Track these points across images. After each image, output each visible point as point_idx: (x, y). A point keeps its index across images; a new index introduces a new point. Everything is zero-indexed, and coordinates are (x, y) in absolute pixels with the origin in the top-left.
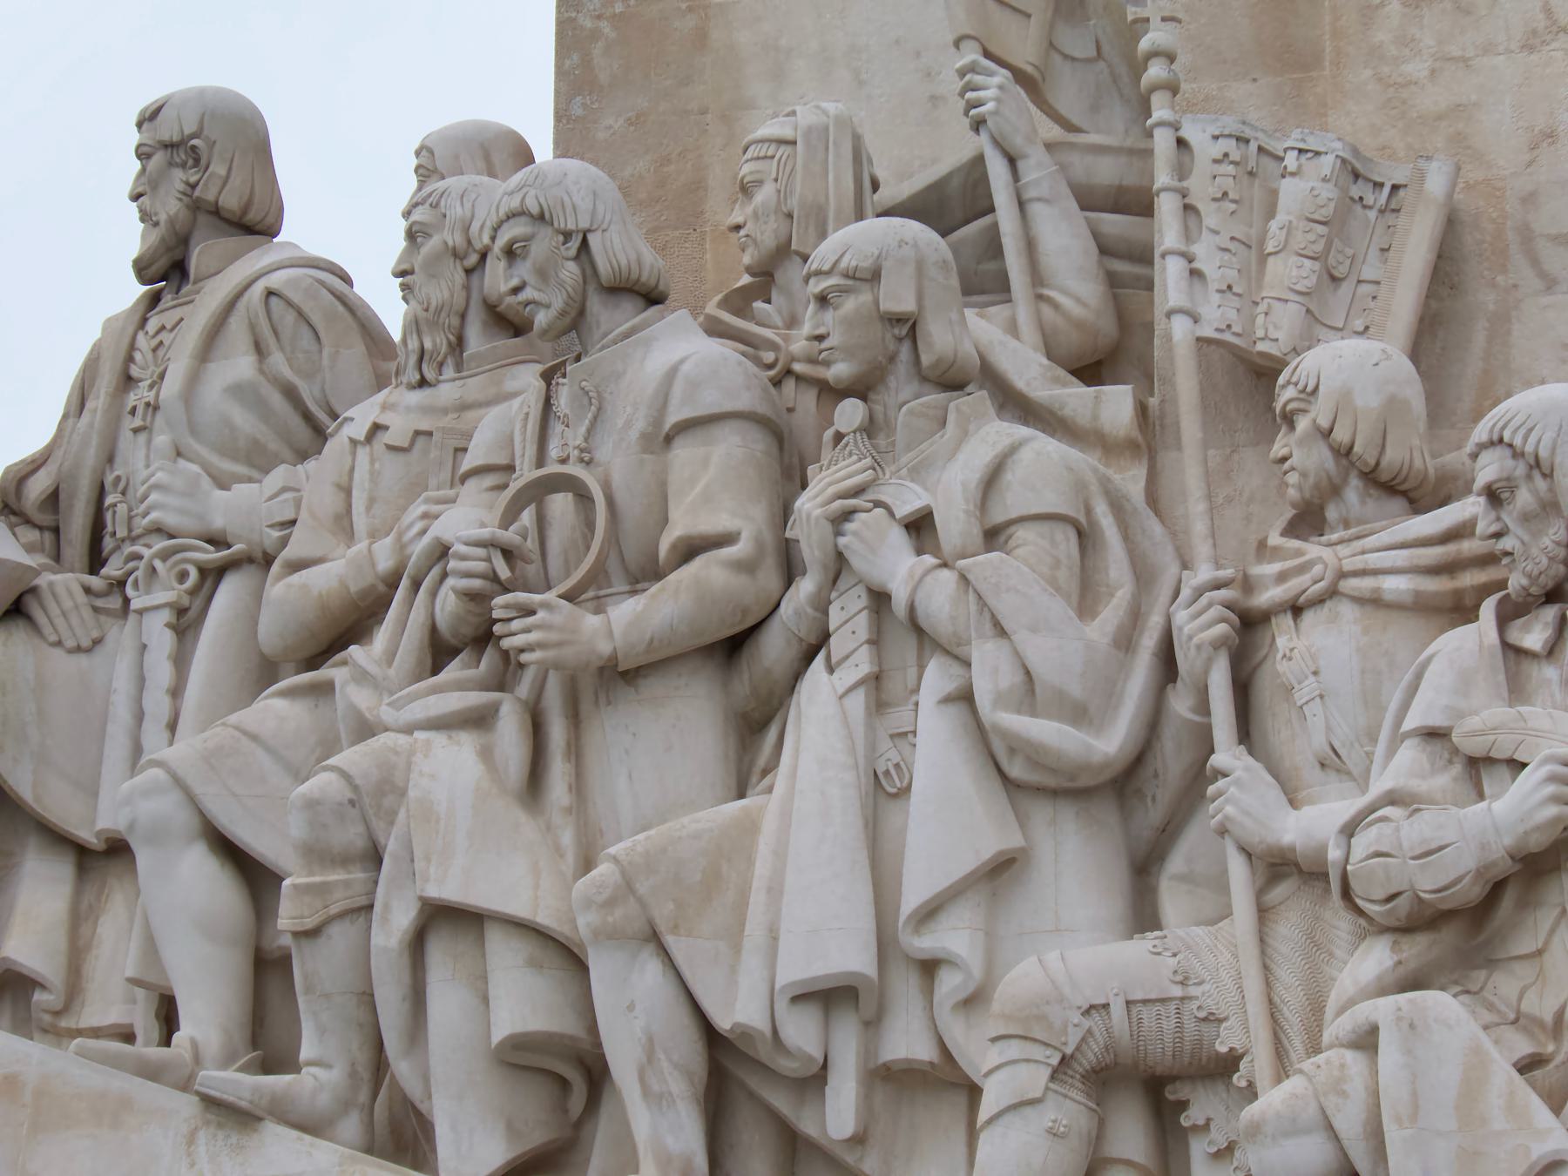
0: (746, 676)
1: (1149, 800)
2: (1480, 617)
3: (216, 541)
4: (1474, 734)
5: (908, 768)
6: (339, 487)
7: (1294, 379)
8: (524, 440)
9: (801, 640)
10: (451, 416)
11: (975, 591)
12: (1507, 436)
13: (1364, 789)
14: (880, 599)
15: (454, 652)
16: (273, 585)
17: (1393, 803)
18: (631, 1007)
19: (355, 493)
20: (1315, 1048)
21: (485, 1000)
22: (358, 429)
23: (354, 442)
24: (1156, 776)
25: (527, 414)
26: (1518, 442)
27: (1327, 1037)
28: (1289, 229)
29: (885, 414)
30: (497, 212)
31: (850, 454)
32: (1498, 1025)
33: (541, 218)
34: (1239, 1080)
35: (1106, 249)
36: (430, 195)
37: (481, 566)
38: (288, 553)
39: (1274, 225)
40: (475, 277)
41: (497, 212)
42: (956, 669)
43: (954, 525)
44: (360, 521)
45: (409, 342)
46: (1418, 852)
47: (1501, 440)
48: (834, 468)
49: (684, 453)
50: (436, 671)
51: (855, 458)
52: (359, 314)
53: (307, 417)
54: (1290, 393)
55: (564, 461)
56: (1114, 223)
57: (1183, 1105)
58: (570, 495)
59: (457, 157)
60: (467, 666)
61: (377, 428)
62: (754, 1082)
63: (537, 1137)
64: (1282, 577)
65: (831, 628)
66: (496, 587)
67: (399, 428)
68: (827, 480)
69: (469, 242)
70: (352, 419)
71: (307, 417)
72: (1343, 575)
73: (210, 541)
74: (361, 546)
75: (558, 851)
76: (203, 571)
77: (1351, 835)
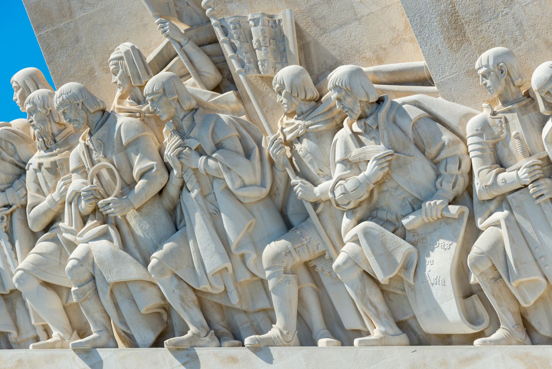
0: (167, 199)
1: (278, 195)
2: (344, 126)
3: (8, 206)
4: (354, 156)
5: (218, 209)
6: (34, 182)
7: (277, 82)
8: (85, 158)
9: (178, 186)
10: (59, 155)
11: (219, 161)
12: (337, 84)
13: (331, 178)
14: (196, 171)
15: (88, 216)
16: (29, 213)
17: (341, 179)
18: (174, 291)
19: (40, 182)
20: (344, 244)
21: (134, 301)
22: (35, 166)
23: (35, 170)
24: (278, 189)
25: (83, 151)
26: (340, 85)
27: (345, 240)
28: (258, 41)
29: (178, 123)
30: (57, 103)
31: (174, 136)
32: (383, 224)
33: (61, 95)
34: (327, 256)
35: (209, 56)
36: (30, 100)
37: (92, 197)
38: (29, 203)
39: (254, 41)
40: (50, 116)
41: (57, 103)
42: (221, 181)
43: (208, 146)
44: (45, 189)
45: (39, 139)
46: (352, 190)
47: (336, 86)
48: (170, 142)
49: (129, 150)
50: (85, 223)
51: (175, 136)
52: (20, 134)
53: (17, 165)
54: (278, 85)
55: (99, 161)
56: (209, 48)
57: (315, 267)
58: (105, 169)
59: (24, 82)
60: (92, 220)
61: (40, 165)
62: (208, 298)
63: (160, 330)
64: (291, 131)
65: (186, 182)
66: (96, 200)
67: (47, 162)
68: (171, 145)
69: (46, 109)
70: (31, 164)
71: (17, 165)
72: (307, 127)
73: (5, 206)
74: (49, 197)
75: (137, 259)
76: (7, 215)
77: (334, 190)
